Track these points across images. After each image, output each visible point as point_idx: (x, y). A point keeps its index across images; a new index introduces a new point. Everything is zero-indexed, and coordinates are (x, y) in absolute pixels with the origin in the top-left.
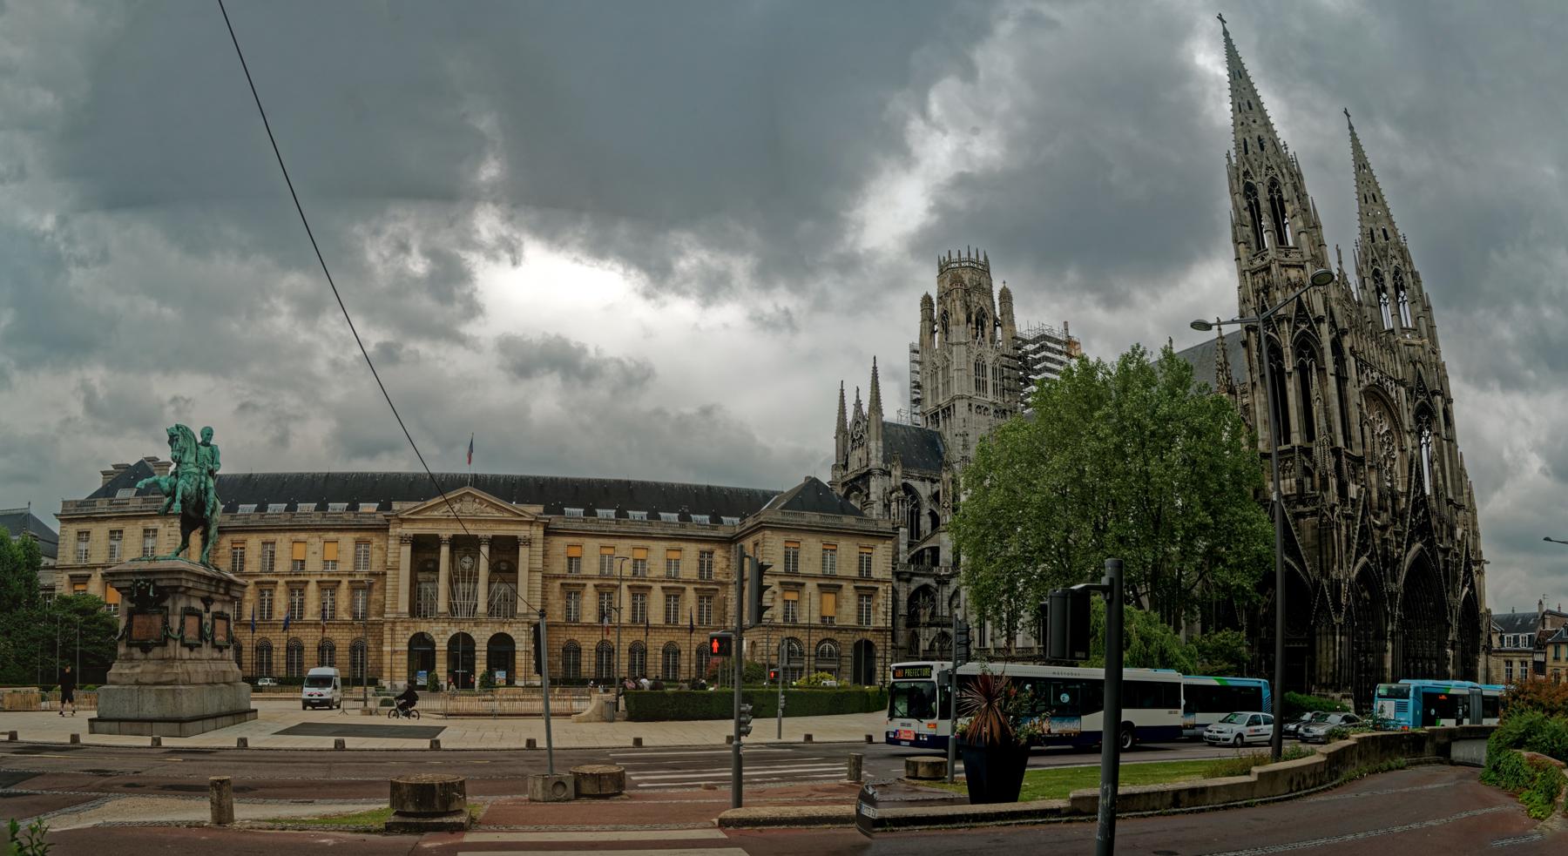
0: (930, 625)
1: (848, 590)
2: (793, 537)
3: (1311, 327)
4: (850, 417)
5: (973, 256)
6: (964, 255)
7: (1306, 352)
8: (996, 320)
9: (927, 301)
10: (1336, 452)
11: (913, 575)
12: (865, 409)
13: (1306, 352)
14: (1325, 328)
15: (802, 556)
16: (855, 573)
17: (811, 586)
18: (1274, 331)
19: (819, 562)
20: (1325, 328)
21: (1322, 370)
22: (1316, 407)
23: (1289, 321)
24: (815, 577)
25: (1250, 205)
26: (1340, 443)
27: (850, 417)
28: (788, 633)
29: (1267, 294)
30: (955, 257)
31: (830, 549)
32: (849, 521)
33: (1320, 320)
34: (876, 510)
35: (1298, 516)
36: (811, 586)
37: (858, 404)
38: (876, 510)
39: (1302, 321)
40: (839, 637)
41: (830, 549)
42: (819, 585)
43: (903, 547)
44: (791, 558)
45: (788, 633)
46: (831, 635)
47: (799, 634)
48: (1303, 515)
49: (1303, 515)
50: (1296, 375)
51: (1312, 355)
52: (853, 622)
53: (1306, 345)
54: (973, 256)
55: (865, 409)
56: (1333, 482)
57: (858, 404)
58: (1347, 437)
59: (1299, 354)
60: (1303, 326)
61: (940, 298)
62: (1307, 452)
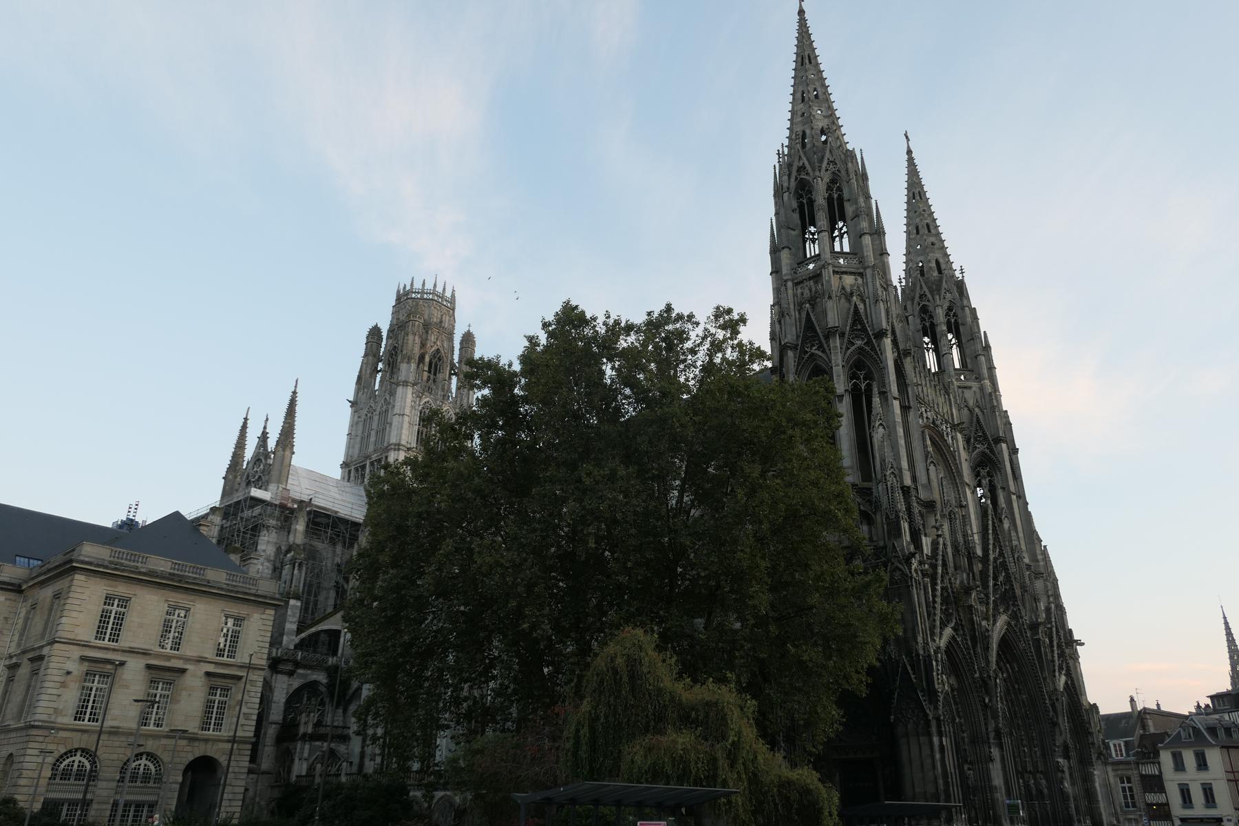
0: (313, 737)
2: (122, 589)
3: (869, 343)
4: (249, 454)
7: (862, 374)
8: (452, 366)
9: (375, 333)
10: (906, 491)
11: (298, 665)
12: (271, 444)
13: (862, 374)
14: (888, 342)
15: (133, 618)
18: (821, 347)
20: (888, 342)
21: (884, 394)
22: (879, 434)
23: (842, 335)
24: (145, 653)
25: (801, 206)
26: (908, 481)
27: (249, 454)
29: (813, 306)
32: (217, 576)
33: (881, 334)
34: (260, 567)
37: (264, 437)
38: (260, 567)
39: (857, 337)
43: (291, 626)
44: (110, 623)
50: (847, 400)
51: (869, 377)
53: (864, 367)
55: (271, 444)
56: (905, 526)
57: (264, 437)
58: (914, 479)
59: (853, 376)
60: (859, 343)
61: (391, 331)
62: (865, 493)
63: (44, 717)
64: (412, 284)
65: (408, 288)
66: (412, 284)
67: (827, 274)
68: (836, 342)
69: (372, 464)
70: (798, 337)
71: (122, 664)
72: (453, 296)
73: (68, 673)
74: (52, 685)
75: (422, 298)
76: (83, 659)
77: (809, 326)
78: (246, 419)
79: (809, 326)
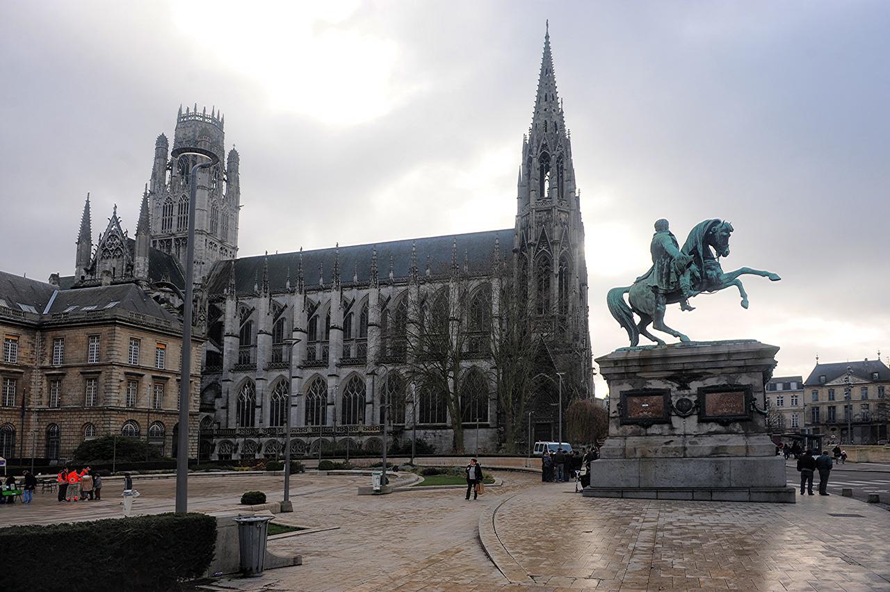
1: (172, 384)
5: (216, 116)
6: (208, 113)
9: (162, 141)
16: (177, 370)
17: (148, 376)
19: (153, 358)
24: (151, 370)
27: (99, 229)
28: (130, 416)
30: (200, 111)
31: (162, 348)
35: (556, 353)
36: (148, 376)
37: (115, 220)
40: (165, 420)
41: (162, 348)
42: (153, 377)
45: (130, 416)
46: (160, 418)
47: (136, 417)
48: (558, 353)
49: (558, 353)
52: (174, 408)
54: (216, 116)
57: (115, 220)
60: (565, 249)
63: (115, 405)
64: (195, 109)
65: (192, 111)
66: (195, 109)
67: (555, 212)
68: (556, 248)
69: (177, 240)
70: (536, 240)
71: (142, 376)
72: (223, 119)
73: (121, 381)
74: (115, 387)
75: (203, 121)
76: (126, 374)
77: (543, 236)
78: (88, 202)
79: (543, 236)
